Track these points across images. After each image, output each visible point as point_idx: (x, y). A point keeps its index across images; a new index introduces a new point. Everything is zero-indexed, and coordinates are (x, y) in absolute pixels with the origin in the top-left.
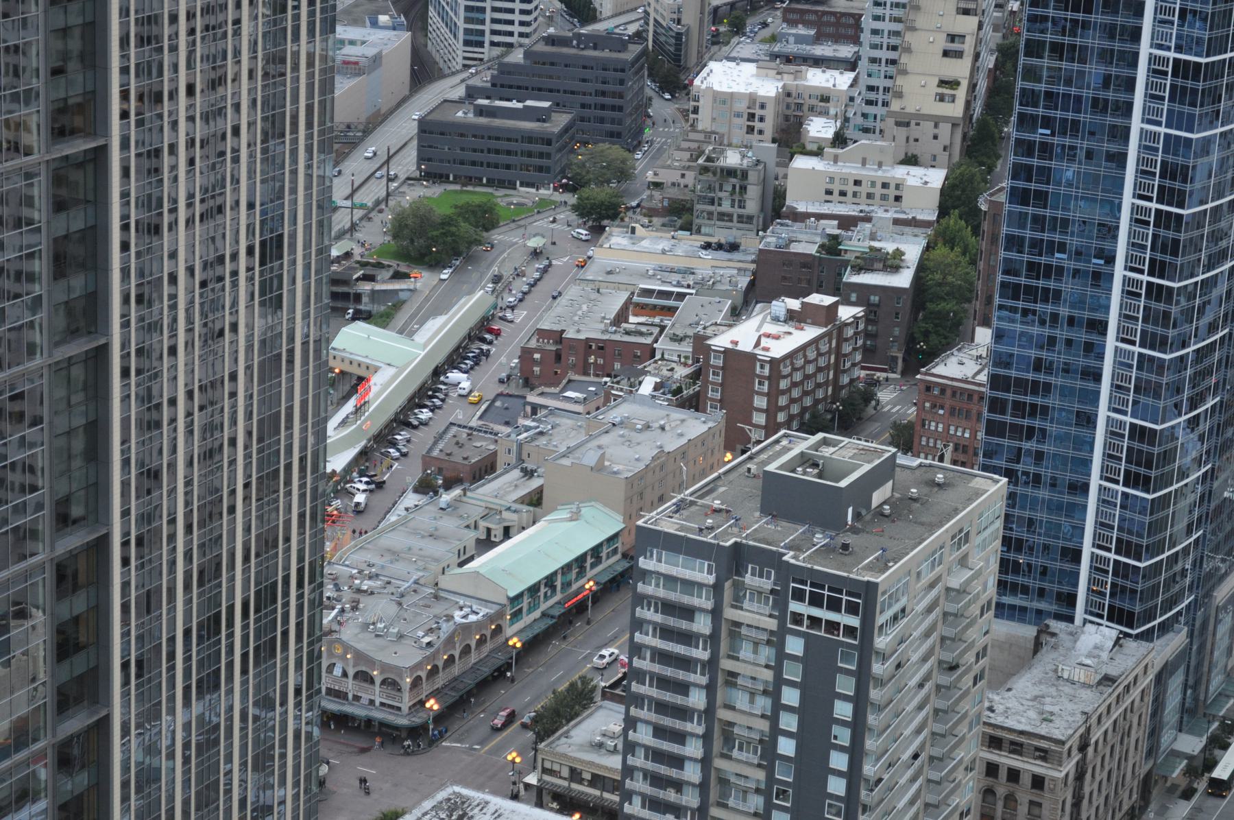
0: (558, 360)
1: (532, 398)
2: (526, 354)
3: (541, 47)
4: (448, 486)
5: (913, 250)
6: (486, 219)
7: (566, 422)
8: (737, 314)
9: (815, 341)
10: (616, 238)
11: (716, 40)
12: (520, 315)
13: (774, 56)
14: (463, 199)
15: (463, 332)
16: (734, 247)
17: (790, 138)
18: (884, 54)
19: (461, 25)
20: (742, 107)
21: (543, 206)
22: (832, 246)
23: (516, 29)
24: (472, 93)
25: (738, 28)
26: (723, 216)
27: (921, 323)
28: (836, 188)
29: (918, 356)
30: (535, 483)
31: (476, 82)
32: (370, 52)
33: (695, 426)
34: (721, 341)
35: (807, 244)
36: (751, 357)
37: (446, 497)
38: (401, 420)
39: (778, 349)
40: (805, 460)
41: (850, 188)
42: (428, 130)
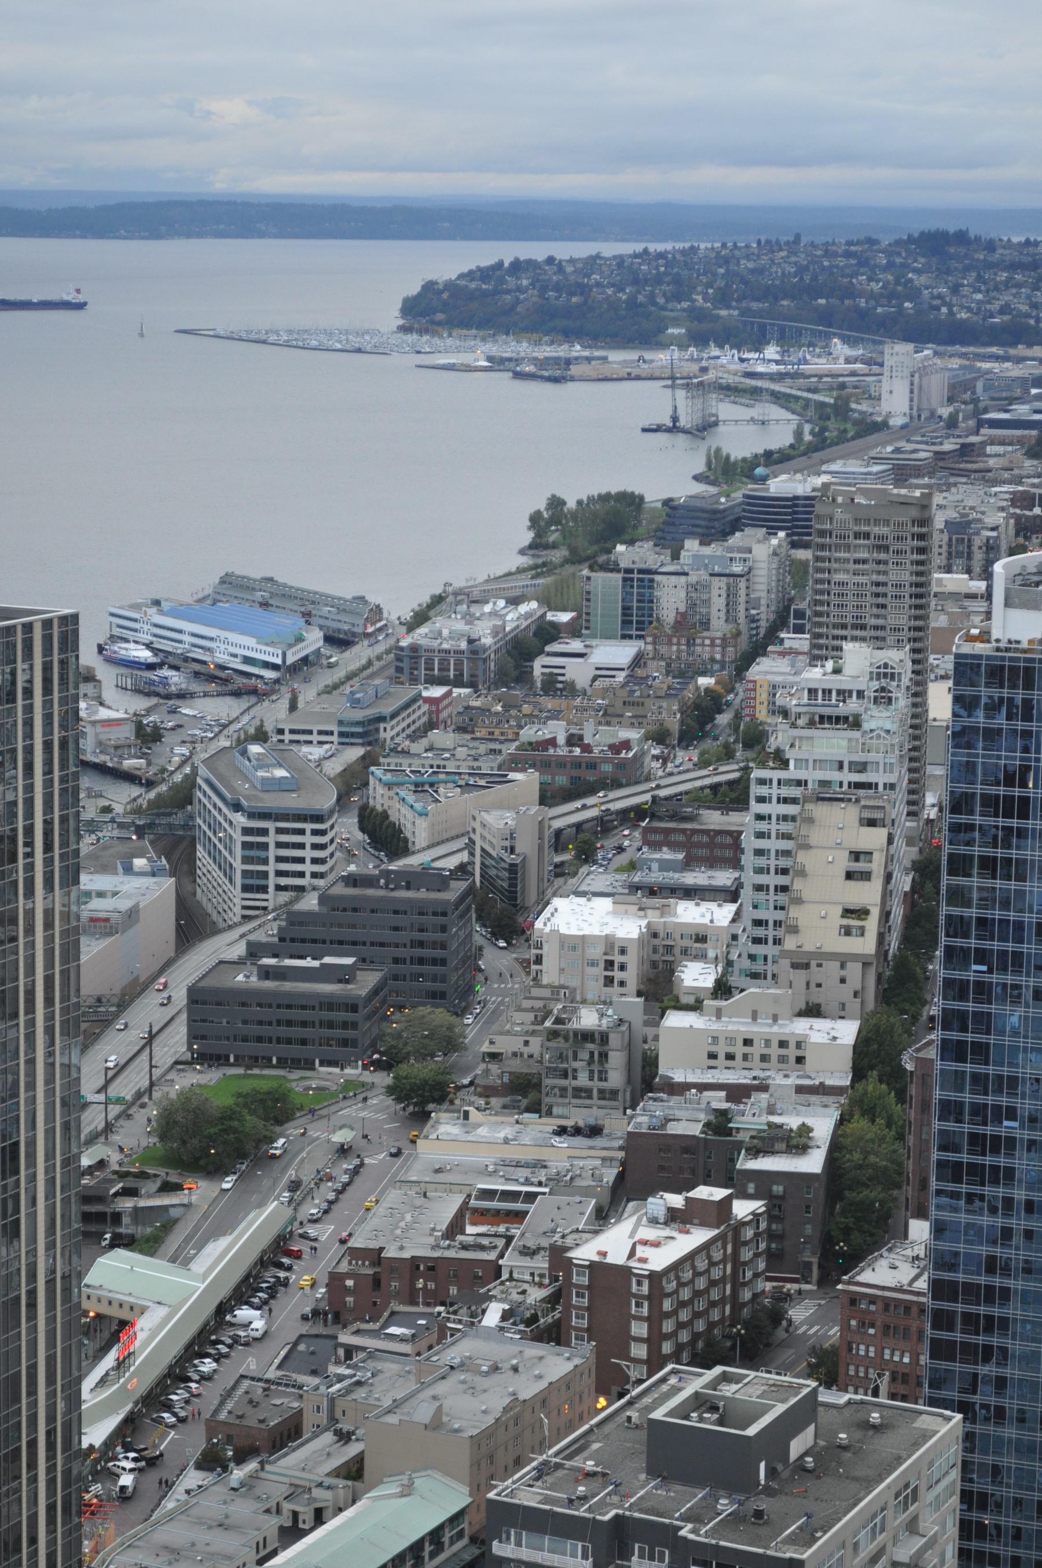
0: (375, 1287)
1: (346, 1338)
2: (335, 1281)
3: (340, 890)
4: (240, 1459)
5: (823, 1125)
6: (278, 1110)
7: (390, 1368)
8: (603, 1217)
9: (706, 1247)
10: (445, 1126)
11: (560, 871)
12: (324, 1232)
13: (634, 888)
14: (248, 1086)
15: (253, 1256)
16: (595, 1131)
17: (660, 990)
18: (772, 880)
19: (238, 866)
20: (596, 952)
21: (353, 1090)
22: (720, 1124)
23: (308, 868)
24: (254, 951)
25: (586, 855)
26: (580, 1093)
27: (842, 1215)
28: (721, 1050)
29: (840, 1257)
30: (353, 1449)
31: (260, 936)
32: (124, 905)
33: (557, 1364)
34: (585, 1253)
35: (688, 1124)
36: (624, 1272)
37: (238, 1474)
38: (176, 1374)
39: (659, 1260)
40: (700, 1402)
41: (739, 1050)
42: (200, 998)
